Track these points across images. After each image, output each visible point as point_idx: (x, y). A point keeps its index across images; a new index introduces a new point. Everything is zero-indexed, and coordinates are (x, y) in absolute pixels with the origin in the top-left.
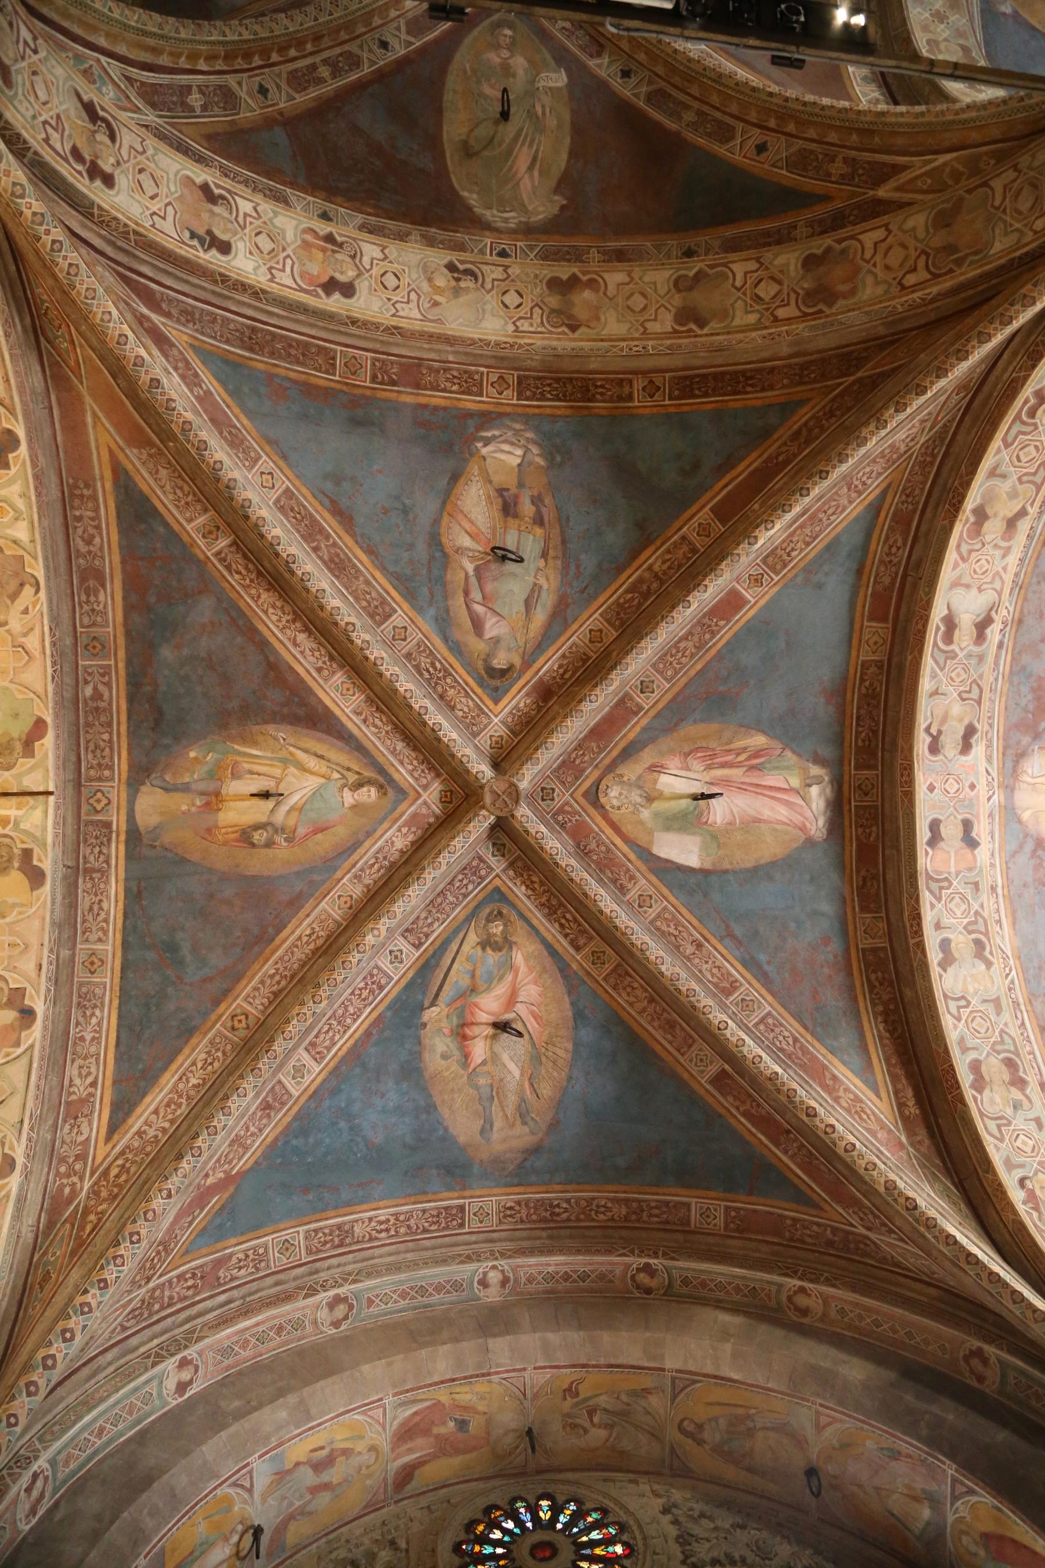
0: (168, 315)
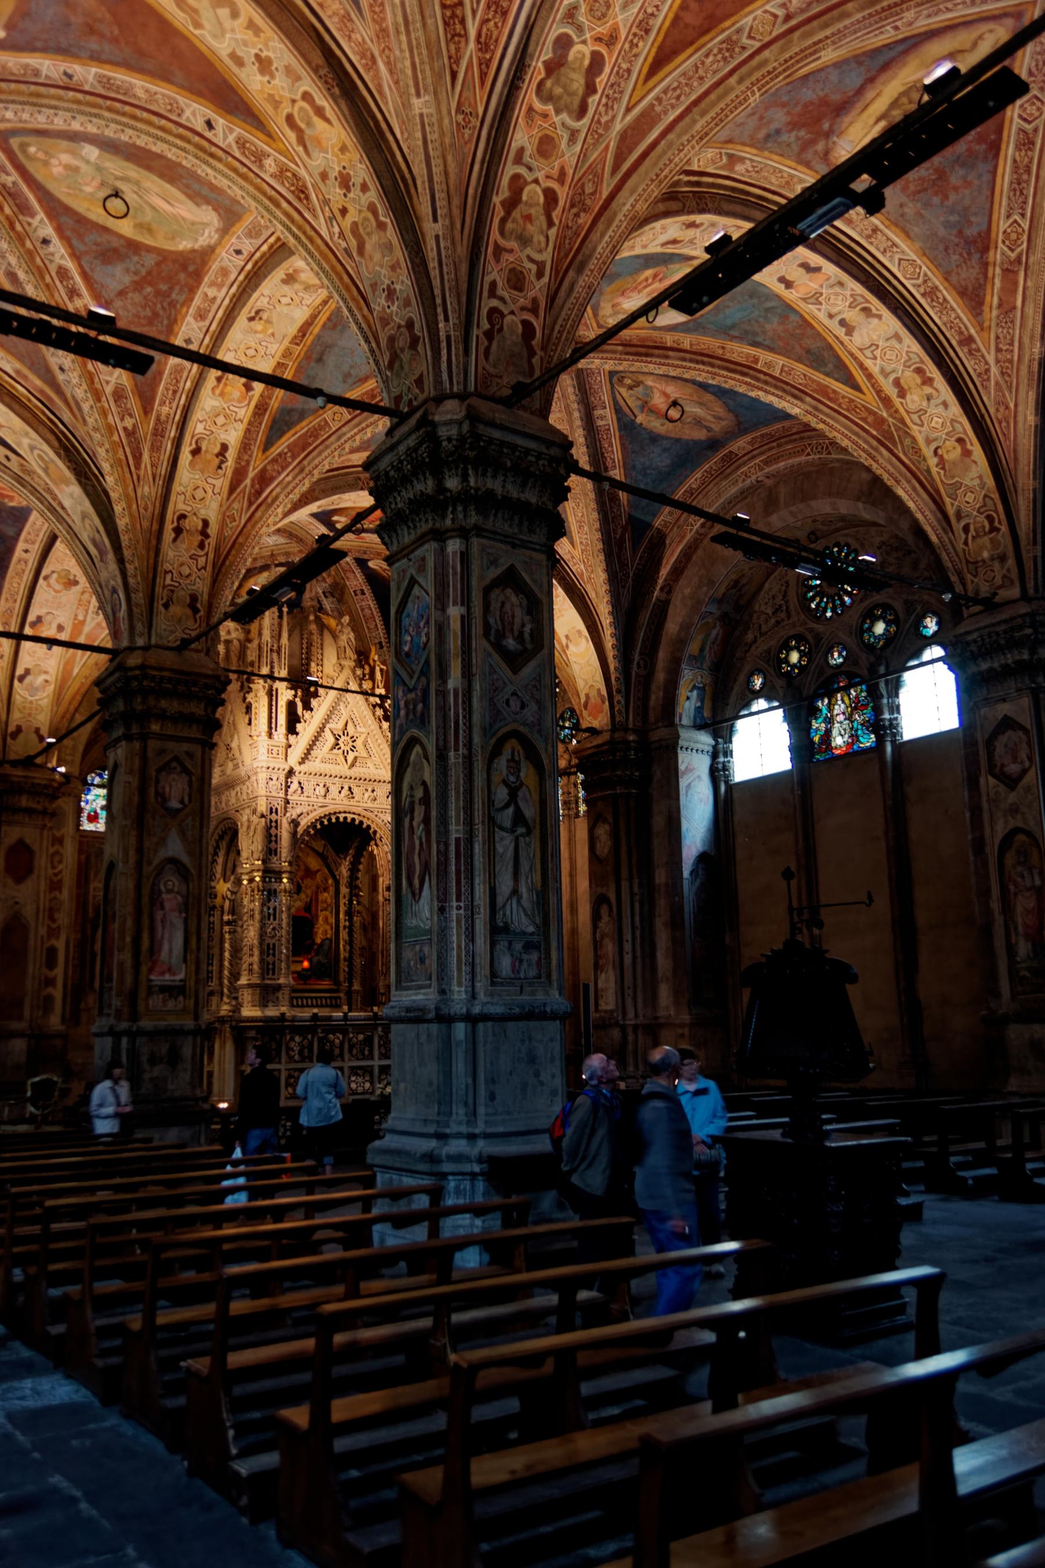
0: (248, 463)
